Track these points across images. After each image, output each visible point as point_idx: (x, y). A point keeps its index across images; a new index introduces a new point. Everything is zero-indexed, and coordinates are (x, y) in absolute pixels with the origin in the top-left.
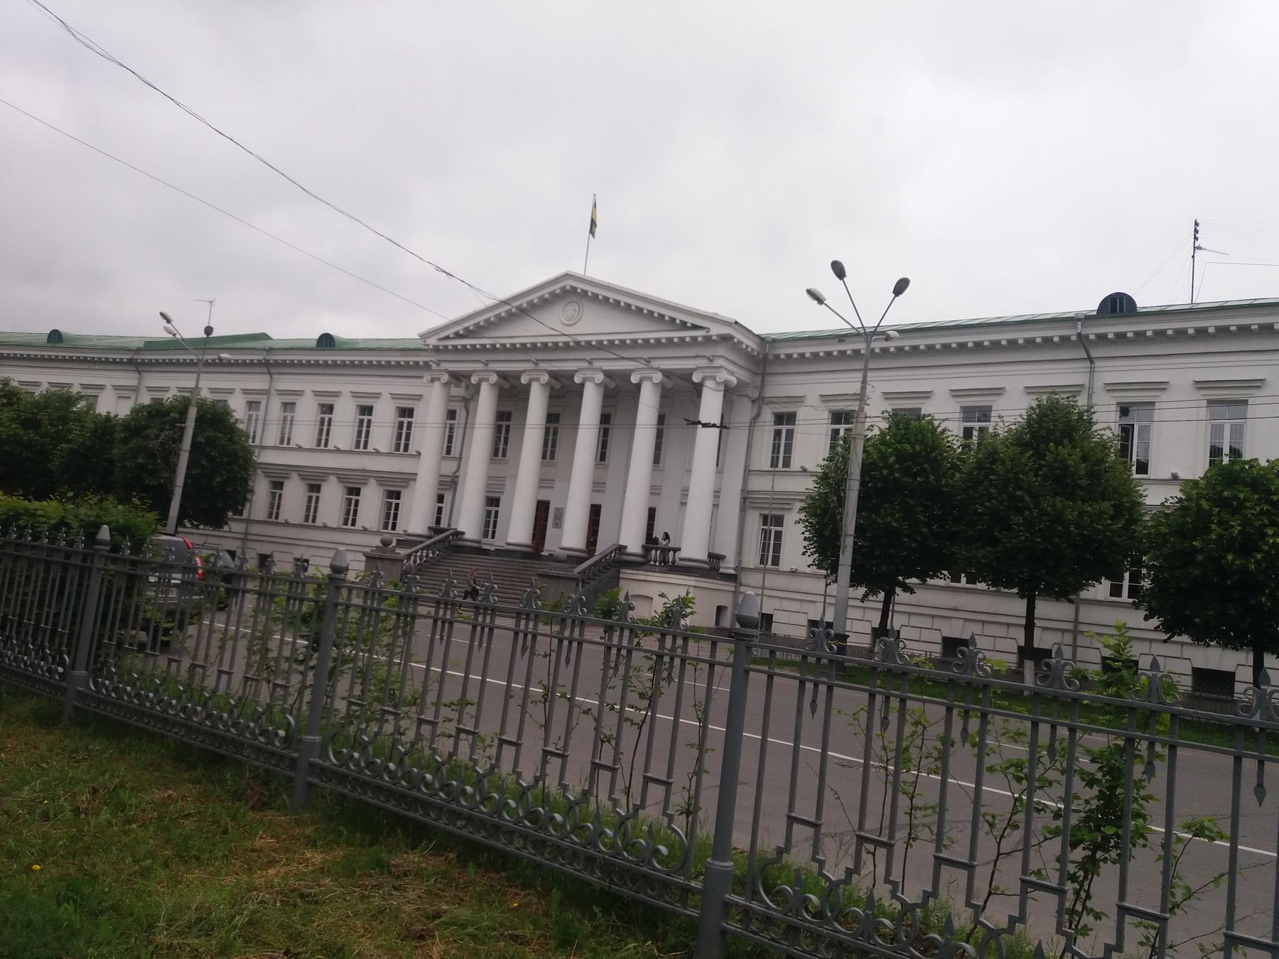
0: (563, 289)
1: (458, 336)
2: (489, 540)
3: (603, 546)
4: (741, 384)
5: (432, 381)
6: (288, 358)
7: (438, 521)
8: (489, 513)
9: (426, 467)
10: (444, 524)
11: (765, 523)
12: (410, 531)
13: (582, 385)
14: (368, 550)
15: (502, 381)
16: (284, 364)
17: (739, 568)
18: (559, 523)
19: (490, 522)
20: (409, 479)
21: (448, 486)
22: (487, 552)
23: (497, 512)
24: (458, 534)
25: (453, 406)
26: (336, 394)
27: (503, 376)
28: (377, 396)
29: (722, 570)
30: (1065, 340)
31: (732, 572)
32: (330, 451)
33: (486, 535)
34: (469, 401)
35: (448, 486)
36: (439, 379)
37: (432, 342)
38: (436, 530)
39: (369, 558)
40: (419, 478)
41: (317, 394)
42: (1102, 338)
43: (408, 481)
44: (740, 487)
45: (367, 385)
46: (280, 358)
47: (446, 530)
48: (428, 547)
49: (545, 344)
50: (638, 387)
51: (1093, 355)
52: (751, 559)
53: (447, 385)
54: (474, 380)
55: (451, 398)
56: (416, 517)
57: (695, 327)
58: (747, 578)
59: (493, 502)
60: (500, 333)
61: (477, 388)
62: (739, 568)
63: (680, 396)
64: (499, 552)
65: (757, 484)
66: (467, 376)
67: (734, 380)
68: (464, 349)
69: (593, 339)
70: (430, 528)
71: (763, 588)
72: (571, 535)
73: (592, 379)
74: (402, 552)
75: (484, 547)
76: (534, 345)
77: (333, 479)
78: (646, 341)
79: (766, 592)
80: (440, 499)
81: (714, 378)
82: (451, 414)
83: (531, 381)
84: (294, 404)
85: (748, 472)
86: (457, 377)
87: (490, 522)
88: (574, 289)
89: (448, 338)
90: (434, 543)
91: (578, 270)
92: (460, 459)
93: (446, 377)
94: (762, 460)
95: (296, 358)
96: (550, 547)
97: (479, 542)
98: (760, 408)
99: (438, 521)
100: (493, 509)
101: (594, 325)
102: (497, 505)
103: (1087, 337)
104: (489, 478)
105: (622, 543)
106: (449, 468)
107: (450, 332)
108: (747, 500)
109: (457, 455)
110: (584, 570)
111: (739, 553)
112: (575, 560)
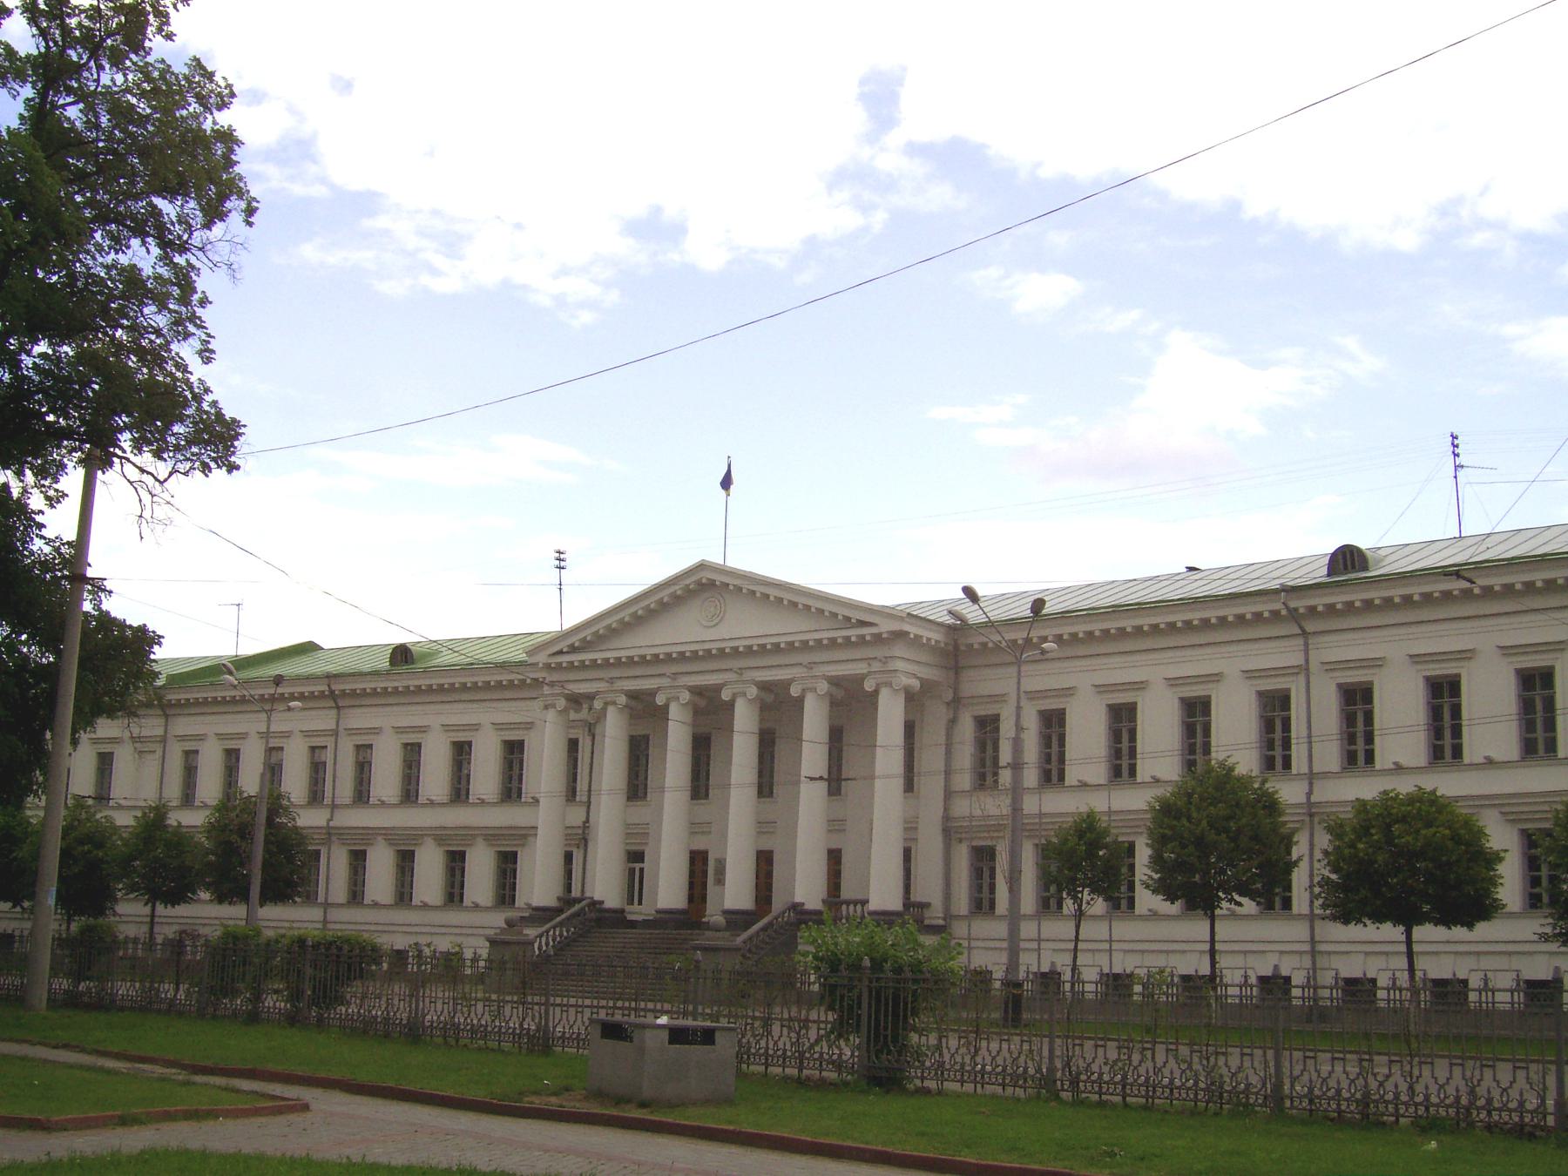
0: (699, 583)
1: (573, 649)
2: (636, 907)
3: (778, 904)
4: (927, 687)
5: (546, 707)
6: (358, 686)
7: (568, 888)
8: (632, 871)
9: (546, 817)
10: (576, 893)
11: (1044, 858)
12: (535, 903)
13: (876, 692)
14: (491, 932)
15: (633, 703)
16: (353, 694)
17: (949, 916)
18: (720, 881)
19: (635, 883)
20: (526, 834)
21: (578, 841)
22: (633, 924)
23: (642, 870)
24: (595, 904)
25: (573, 734)
26: (423, 729)
27: (697, 691)
28: (475, 727)
29: (927, 922)
30: (1275, 614)
31: (941, 922)
32: (374, 806)
33: (631, 902)
34: (591, 729)
35: (578, 841)
36: (554, 706)
37: (542, 658)
38: (567, 901)
39: (493, 942)
40: (540, 832)
41: (399, 730)
42: (1312, 610)
43: (525, 836)
44: (940, 813)
45: (459, 714)
46: (348, 687)
47: (579, 900)
48: (561, 924)
49: (682, 654)
50: (800, 701)
51: (1309, 628)
52: (962, 903)
53: (565, 711)
54: (598, 704)
55: (571, 724)
56: (539, 884)
57: (862, 624)
58: (959, 929)
59: (636, 856)
60: (616, 643)
61: (604, 710)
62: (949, 916)
63: (851, 706)
64: (647, 924)
65: (961, 807)
66: (591, 697)
67: (916, 684)
68: (583, 666)
69: (741, 644)
70: (559, 899)
71: (1039, 940)
72: (735, 892)
73: (744, 694)
74: (531, 932)
75: (630, 917)
76: (669, 655)
77: (430, 842)
78: (819, 641)
79: (974, 944)
80: (568, 858)
81: (889, 685)
82: (573, 745)
83: (669, 700)
84: (370, 746)
85: (949, 794)
86: (575, 701)
87: (635, 883)
88: (712, 583)
89: (561, 652)
90: (568, 919)
91: (716, 558)
92: (589, 803)
93: (561, 703)
94: (964, 781)
95: (369, 685)
96: (713, 915)
97: (622, 911)
98: (955, 713)
99: (568, 888)
100: (637, 866)
101: (743, 625)
102: (642, 861)
103: (1296, 610)
104: (628, 825)
105: (798, 899)
106: (576, 816)
107: (563, 646)
108: (949, 832)
109: (585, 799)
110: (750, 938)
111: (947, 896)
112: (738, 920)
